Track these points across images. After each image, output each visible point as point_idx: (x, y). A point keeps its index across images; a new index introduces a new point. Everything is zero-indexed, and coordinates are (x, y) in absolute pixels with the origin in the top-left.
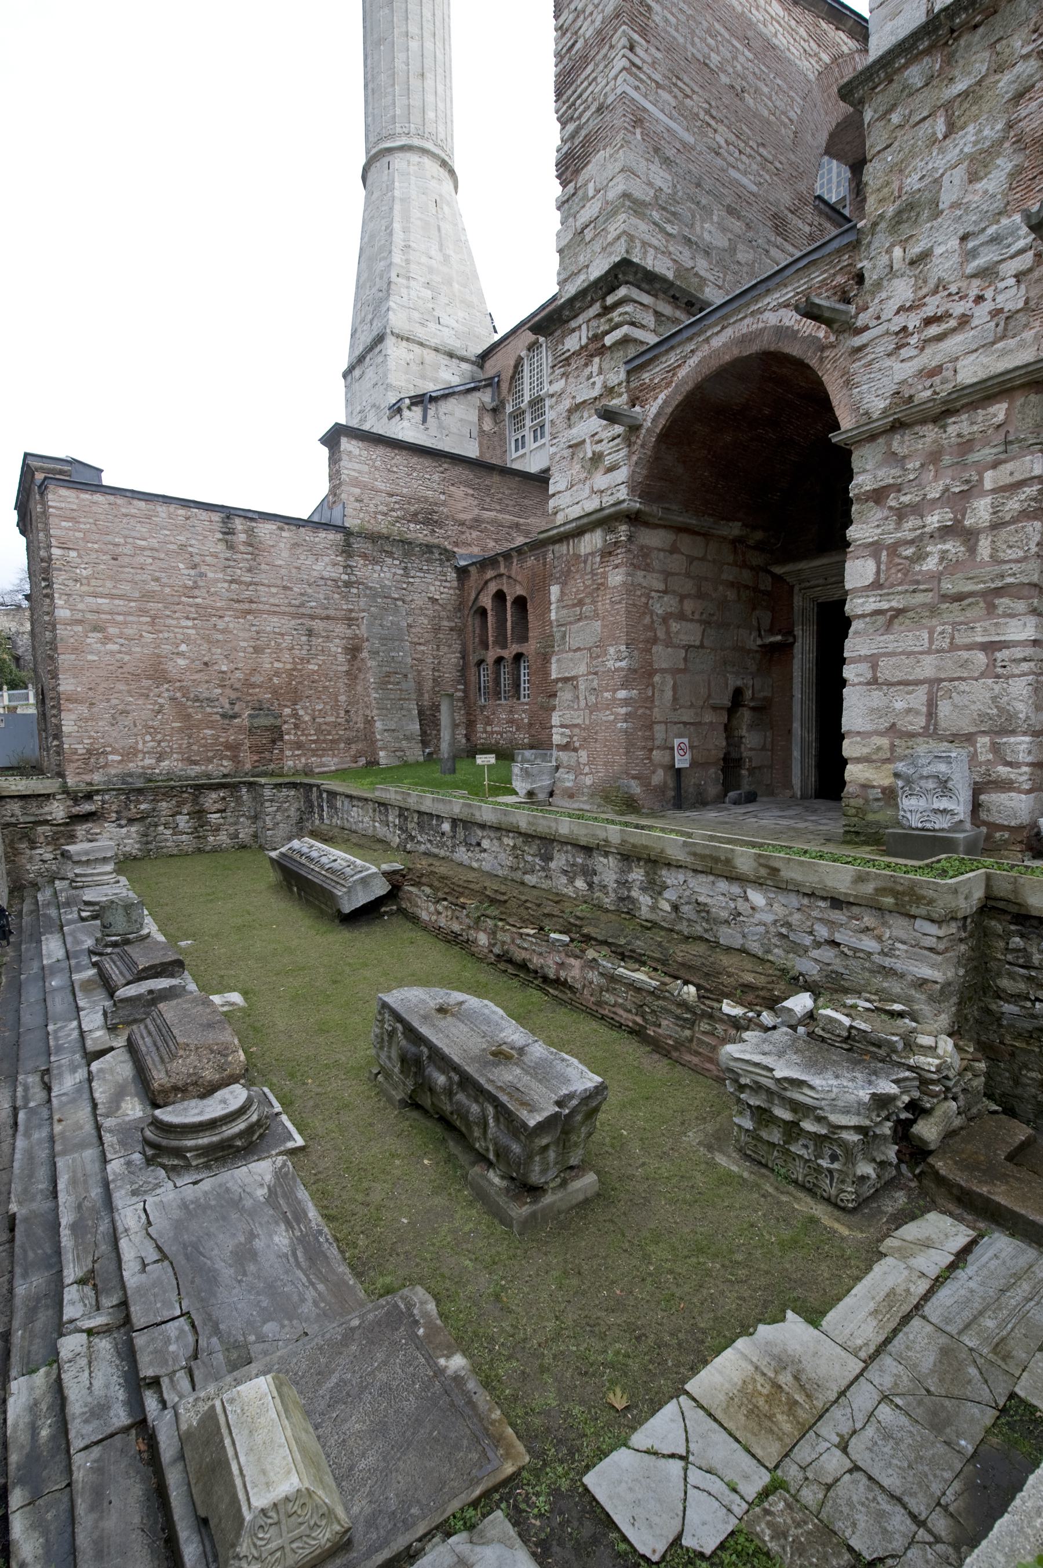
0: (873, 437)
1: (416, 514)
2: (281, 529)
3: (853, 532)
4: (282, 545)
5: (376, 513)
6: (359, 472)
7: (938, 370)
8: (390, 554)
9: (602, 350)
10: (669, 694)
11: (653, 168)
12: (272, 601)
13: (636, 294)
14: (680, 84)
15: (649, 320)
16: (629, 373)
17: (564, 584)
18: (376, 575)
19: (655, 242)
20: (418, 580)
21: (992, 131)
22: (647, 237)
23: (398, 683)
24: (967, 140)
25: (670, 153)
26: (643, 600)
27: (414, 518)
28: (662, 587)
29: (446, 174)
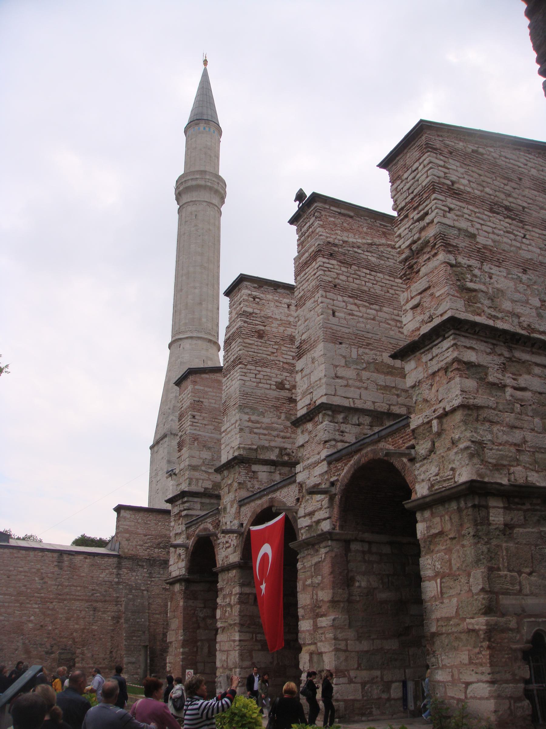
0: (220, 572)
1: (159, 544)
2: (86, 558)
3: (219, 600)
4: (85, 566)
5: (136, 545)
6: (129, 526)
7: (227, 557)
8: (142, 566)
9: (181, 516)
10: (206, 650)
11: (202, 452)
12: (77, 594)
13: (191, 499)
14: (216, 420)
15: (198, 506)
16: (187, 528)
17: (171, 602)
18: (133, 578)
19: (202, 477)
20: (157, 579)
21: (233, 497)
22: (198, 477)
23: (139, 636)
24: (231, 496)
25: (211, 445)
26: (193, 611)
27: (158, 546)
28: (202, 605)
29: (212, 345)
